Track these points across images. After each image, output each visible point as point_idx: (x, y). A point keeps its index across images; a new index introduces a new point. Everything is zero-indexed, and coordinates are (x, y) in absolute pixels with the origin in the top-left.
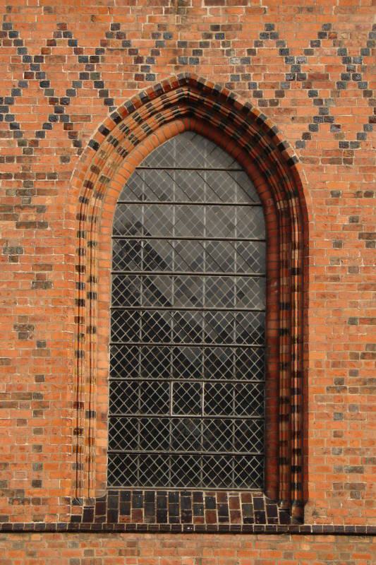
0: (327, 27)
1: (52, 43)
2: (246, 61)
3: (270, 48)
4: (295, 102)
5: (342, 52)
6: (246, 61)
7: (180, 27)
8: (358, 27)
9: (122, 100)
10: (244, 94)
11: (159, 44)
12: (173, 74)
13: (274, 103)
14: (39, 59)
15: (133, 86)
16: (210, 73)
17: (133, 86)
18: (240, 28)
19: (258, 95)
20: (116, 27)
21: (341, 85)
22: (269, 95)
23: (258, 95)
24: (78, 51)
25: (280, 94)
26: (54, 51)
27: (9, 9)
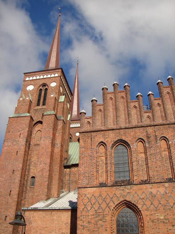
0: (144, 191)
1: (106, 196)
3: (136, 195)
4: (140, 202)
5: (146, 195)
9: (116, 203)
10: (133, 201)
12: (123, 199)
14: (105, 198)
16: (128, 199)
18: (131, 192)
19: (135, 201)
20: (115, 193)
23: (135, 201)
25: (138, 201)
26: (107, 197)
27: (100, 192)
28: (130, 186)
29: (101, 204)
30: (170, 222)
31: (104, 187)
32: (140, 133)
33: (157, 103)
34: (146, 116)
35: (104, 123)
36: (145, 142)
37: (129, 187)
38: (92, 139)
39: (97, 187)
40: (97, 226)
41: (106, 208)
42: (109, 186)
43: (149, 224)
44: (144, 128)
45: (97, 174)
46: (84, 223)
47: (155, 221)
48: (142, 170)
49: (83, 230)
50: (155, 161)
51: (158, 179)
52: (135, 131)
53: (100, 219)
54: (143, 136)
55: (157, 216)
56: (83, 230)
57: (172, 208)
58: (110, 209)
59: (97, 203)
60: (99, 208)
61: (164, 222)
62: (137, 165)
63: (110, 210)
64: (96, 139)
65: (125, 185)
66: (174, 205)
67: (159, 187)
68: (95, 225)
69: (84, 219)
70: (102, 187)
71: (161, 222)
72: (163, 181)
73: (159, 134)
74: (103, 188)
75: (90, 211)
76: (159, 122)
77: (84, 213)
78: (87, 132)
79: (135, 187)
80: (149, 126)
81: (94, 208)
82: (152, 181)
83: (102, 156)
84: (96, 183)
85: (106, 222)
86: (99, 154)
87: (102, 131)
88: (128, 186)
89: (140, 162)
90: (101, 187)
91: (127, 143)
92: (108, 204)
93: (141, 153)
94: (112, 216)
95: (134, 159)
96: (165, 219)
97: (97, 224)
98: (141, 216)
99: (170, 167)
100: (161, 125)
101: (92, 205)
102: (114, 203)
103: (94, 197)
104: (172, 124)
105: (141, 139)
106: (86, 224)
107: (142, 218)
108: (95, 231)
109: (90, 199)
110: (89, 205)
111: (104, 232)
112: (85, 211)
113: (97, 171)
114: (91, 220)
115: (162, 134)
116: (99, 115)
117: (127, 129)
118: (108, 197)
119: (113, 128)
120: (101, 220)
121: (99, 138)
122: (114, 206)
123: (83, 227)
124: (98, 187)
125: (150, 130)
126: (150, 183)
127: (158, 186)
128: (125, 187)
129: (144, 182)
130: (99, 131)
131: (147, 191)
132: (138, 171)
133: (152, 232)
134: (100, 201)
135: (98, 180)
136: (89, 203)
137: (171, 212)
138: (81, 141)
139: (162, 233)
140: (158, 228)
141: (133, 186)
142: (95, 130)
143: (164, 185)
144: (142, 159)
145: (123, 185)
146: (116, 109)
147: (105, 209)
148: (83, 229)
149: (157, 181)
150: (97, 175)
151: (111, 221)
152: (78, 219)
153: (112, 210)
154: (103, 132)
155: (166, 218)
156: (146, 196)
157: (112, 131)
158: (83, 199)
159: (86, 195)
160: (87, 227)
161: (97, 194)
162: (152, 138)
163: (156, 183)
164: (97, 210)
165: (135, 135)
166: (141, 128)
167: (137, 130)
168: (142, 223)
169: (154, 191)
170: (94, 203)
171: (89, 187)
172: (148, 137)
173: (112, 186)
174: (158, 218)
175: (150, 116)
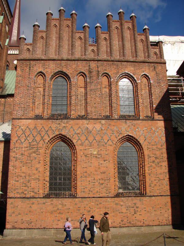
0: (80, 126)
4: (75, 137)
5: (82, 130)
8: (84, 127)
10: (68, 136)
12: (58, 133)
13: (72, 137)
16: (63, 133)
18: (67, 127)
19: (70, 136)
20: (50, 126)
24: (45, 130)
25: (73, 136)
27: (36, 124)
28: (67, 120)
29: (35, 137)
30: (102, 157)
31: (39, 119)
32: (82, 67)
33: (104, 37)
34: (91, 50)
35: (46, 52)
36: (86, 76)
38: (30, 68)
39: (32, 119)
40: (30, 158)
42: (45, 119)
43: (82, 158)
44: (87, 61)
45: (33, 105)
46: (17, 154)
47: (88, 156)
48: (80, 105)
49: (16, 162)
50: (95, 97)
51: (95, 115)
52: (77, 63)
53: (33, 152)
54: (85, 70)
55: (91, 151)
56: (16, 162)
57: (106, 144)
58: (44, 142)
59: (31, 136)
60: (33, 140)
61: (96, 157)
62: (76, 99)
64: (35, 68)
65: (61, 119)
66: (108, 142)
67: (96, 123)
68: (28, 157)
69: (18, 151)
70: (38, 119)
71: (93, 157)
72: (100, 117)
73: (102, 70)
74: (38, 120)
76: (103, 58)
77: (17, 145)
78: (26, 60)
79: (71, 122)
80: (92, 60)
81: (28, 140)
82: (90, 117)
83: (40, 87)
84: (31, 115)
85: (40, 154)
86: (37, 85)
87: (42, 60)
88: (65, 120)
89: (79, 97)
90: (36, 119)
91: (68, 75)
92: (43, 137)
93: (81, 87)
94: (46, 149)
95: (73, 93)
96: (98, 154)
97: (30, 157)
98: (75, 151)
99: (108, 105)
100: (105, 61)
101: (26, 137)
102: (49, 136)
103: (29, 129)
104: (116, 61)
105: (82, 73)
107: (75, 152)
108: (27, 163)
109: (24, 131)
110: (23, 137)
113: (34, 103)
114: (24, 152)
115: (105, 70)
116: (40, 42)
117: (69, 61)
118: (43, 129)
119: (54, 59)
120: (34, 152)
121: (38, 67)
122: (49, 139)
124: (33, 119)
125: (93, 65)
126: (87, 119)
127: (95, 122)
128: (62, 121)
129: (81, 117)
130: (39, 60)
131: (83, 126)
132: (76, 105)
133: (83, 165)
134: (35, 134)
135: (34, 112)
137: (104, 148)
138: (18, 69)
139: (94, 167)
141: (70, 120)
142: (34, 59)
144: (82, 94)
145: (60, 119)
146: (60, 38)
147: (39, 142)
148: (16, 160)
149: (94, 117)
150: (33, 107)
151: (45, 154)
152: (11, 151)
153: (46, 143)
154: (43, 62)
155: (99, 153)
156: (81, 131)
157: (52, 62)
159: (20, 127)
160: (20, 159)
161: (32, 127)
162: (94, 73)
163: (93, 119)
164: (31, 143)
165: (77, 68)
166: (84, 62)
167: (79, 63)
168: (75, 157)
169: (90, 127)
170: (29, 136)
171: (23, 119)
172: (90, 72)
173: (48, 119)
174: (91, 153)
175: (95, 50)
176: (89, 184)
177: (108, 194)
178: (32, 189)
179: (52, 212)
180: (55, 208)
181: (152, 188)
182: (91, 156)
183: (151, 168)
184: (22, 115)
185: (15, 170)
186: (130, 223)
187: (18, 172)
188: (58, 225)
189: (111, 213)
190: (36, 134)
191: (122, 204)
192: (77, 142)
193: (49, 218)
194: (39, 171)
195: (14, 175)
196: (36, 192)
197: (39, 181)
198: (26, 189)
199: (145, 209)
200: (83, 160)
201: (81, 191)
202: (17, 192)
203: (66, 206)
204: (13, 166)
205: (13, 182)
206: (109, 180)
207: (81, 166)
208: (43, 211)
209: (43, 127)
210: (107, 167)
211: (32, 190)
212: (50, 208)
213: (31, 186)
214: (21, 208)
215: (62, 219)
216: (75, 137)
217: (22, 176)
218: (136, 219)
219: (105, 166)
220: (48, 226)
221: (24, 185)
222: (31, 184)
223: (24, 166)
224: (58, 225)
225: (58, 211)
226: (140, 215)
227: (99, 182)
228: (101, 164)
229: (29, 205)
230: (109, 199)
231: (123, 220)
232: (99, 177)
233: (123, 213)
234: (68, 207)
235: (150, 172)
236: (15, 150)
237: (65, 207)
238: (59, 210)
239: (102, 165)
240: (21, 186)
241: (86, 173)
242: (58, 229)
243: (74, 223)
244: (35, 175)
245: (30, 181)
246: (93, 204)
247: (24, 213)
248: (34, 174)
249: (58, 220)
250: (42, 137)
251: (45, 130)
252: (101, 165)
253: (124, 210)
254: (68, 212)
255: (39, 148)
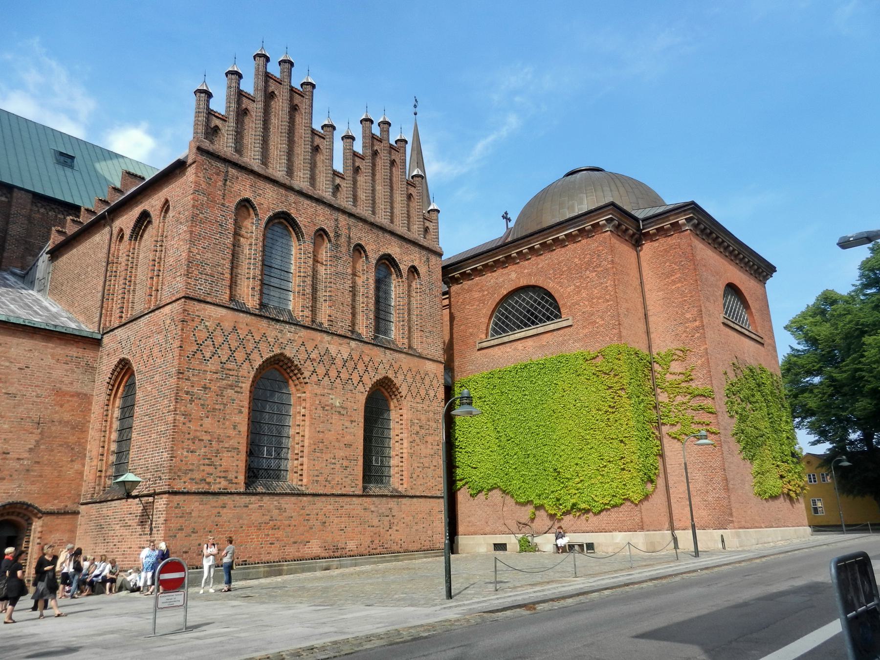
0: (316, 345)
1: (247, 335)
2: (297, 351)
4: (308, 366)
6: (297, 351)
7: (281, 338)
9: (266, 356)
11: (276, 342)
14: (243, 339)
15: (268, 353)
16: (289, 353)
17: (268, 353)
19: (300, 362)
21: (319, 363)
22: (302, 362)
23: (300, 362)
27: (236, 322)
29: (234, 351)
32: (324, 219)
37: (293, 329)
41: (244, 361)
46: (193, 386)
47: (327, 408)
49: (191, 404)
53: (230, 386)
55: (332, 399)
56: (191, 404)
58: (251, 365)
59: (226, 346)
60: (229, 358)
63: (252, 368)
64: (237, 187)
68: (217, 395)
75: (208, 360)
85: (242, 393)
91: (300, 228)
96: (342, 408)
97: (222, 395)
101: (214, 347)
102: (260, 354)
103: (222, 330)
106: (198, 390)
108: (216, 409)
110: (208, 346)
111: (235, 414)
112: (198, 358)
120: (231, 386)
121: (244, 188)
123: (192, 398)
134: (234, 344)
136: (209, 342)
140: (329, 422)
143: (349, 344)
148: (192, 401)
153: (255, 370)
158: (195, 329)
160: (200, 399)
161: (227, 325)
164: (225, 363)
165: (315, 218)
167: (320, 209)
169: (333, 350)
170: (220, 346)
176: (326, 466)
177: (353, 489)
178: (224, 471)
179: (260, 526)
180: (267, 515)
181: (414, 482)
182: (332, 408)
183: (413, 444)
184: (208, 294)
185: (188, 424)
186: (382, 546)
187: (196, 431)
188: (271, 553)
189: (357, 527)
190: (237, 344)
191: (372, 509)
192: (310, 376)
193: (254, 539)
194: (240, 432)
195: (187, 436)
196: (232, 480)
197: (237, 454)
198: (211, 472)
199: (404, 521)
200: (319, 417)
201: (313, 480)
202: (190, 479)
203: (285, 511)
204: (183, 415)
205: (182, 454)
206: (356, 460)
207: (315, 428)
208: (244, 524)
209: (250, 330)
210: (354, 436)
211: (223, 474)
212: (256, 517)
213: (221, 465)
214: (199, 517)
215: (278, 540)
216: (308, 366)
217: (203, 440)
218: (392, 537)
219: (351, 433)
220: (251, 557)
221: (207, 461)
222: (221, 460)
223: (208, 417)
224: (271, 553)
225: (271, 522)
226: (397, 531)
227: (342, 464)
228: (346, 428)
229: (215, 511)
230: (354, 499)
231: (373, 541)
232: (342, 454)
233: (373, 526)
234: (290, 515)
235: (412, 452)
236: (190, 374)
237: (284, 514)
238: (273, 520)
239: (348, 430)
240: (200, 464)
241: (323, 443)
242: (271, 562)
243: (299, 549)
244: (231, 439)
245: (219, 453)
246: (330, 507)
247: (205, 529)
248: (229, 437)
249: (270, 544)
250: (248, 355)
251: (254, 339)
252: (346, 430)
253: (375, 522)
254: (290, 526)
255: (241, 379)
